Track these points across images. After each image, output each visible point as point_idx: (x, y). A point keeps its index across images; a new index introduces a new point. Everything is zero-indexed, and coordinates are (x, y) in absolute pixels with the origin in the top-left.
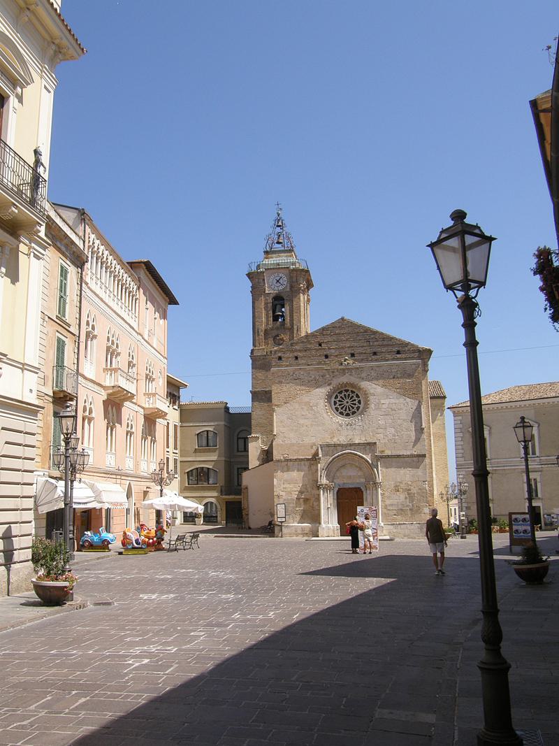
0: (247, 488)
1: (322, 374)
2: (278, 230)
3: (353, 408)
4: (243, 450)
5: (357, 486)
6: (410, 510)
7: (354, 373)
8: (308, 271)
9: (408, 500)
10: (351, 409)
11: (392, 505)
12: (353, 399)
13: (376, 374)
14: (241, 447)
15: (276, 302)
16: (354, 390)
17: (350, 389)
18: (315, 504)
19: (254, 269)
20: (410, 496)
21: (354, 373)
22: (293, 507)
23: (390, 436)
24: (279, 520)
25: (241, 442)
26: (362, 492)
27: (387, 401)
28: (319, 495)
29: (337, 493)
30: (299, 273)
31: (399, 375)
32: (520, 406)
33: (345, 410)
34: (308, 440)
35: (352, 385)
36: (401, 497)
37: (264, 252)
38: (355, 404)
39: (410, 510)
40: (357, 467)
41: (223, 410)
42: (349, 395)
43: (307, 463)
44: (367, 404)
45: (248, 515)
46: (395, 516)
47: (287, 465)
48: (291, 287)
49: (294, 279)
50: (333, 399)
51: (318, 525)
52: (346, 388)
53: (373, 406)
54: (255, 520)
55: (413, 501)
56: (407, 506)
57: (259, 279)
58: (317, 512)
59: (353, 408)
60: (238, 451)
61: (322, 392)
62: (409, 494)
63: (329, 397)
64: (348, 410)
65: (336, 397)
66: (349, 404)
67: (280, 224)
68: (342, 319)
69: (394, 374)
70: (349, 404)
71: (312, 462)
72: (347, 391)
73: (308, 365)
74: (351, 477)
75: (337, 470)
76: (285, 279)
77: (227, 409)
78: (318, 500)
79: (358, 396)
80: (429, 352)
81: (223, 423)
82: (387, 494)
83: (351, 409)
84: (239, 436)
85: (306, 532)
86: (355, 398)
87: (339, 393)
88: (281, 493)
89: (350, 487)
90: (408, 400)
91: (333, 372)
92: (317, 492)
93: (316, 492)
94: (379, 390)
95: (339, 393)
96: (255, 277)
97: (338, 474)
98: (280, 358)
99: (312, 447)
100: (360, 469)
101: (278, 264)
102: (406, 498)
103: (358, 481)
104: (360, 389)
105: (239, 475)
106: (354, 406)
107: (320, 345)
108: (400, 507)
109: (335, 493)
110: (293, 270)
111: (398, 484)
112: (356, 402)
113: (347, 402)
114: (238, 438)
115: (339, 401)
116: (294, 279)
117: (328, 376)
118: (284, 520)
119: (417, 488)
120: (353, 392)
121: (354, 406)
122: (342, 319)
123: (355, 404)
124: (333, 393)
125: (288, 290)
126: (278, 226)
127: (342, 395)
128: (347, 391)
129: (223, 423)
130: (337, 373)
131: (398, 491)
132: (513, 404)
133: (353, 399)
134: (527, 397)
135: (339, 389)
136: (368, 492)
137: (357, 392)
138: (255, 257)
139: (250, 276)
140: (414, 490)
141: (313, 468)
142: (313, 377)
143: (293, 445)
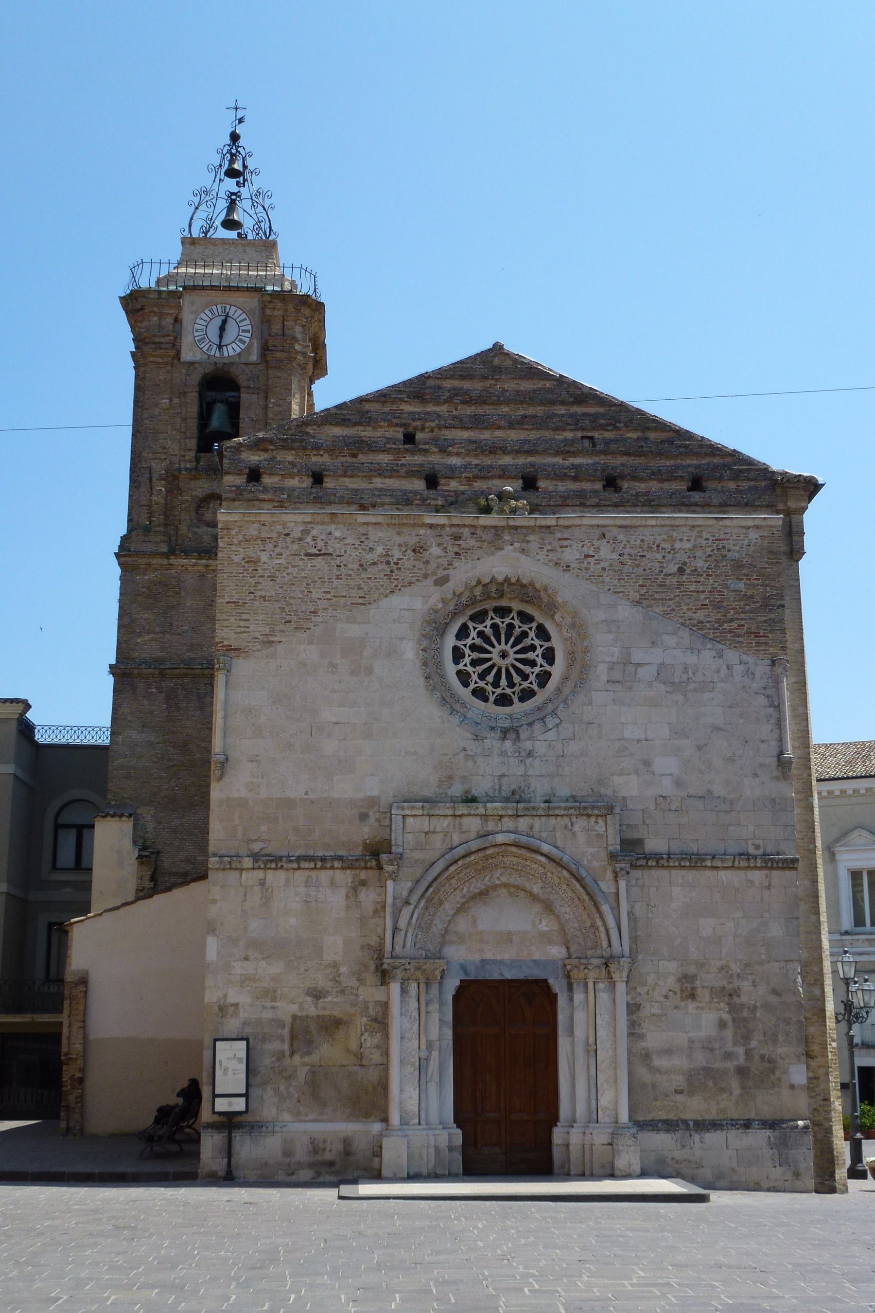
0: (83, 981)
1: (413, 541)
2: (230, 184)
3: (525, 677)
4: (72, 865)
5: (537, 973)
6: (742, 1072)
7: (534, 546)
8: (319, 307)
9: (729, 1033)
10: (517, 679)
11: (668, 1052)
12: (527, 642)
13: (615, 556)
14: (66, 857)
15: (211, 395)
16: (529, 610)
17: (516, 606)
18: (370, 1041)
19: (146, 281)
20: (741, 1021)
21: (534, 546)
22: (280, 1056)
23: (667, 786)
24: (221, 1105)
25: (68, 841)
26: (553, 999)
27: (656, 656)
28: (385, 1006)
29: (456, 998)
30: (290, 307)
31: (700, 564)
32: (854, 791)
33: (496, 684)
34: (344, 789)
35: (526, 591)
36: (704, 1020)
37: (184, 241)
38: (533, 664)
39: (742, 1072)
40: (534, 898)
41: (14, 726)
42: (511, 627)
43: (344, 878)
44: (581, 665)
45: (81, 1080)
46: (679, 1098)
47: (262, 883)
48: (265, 349)
49: (276, 328)
50: (450, 640)
51: (377, 1127)
52: (503, 603)
53: (601, 672)
54: (114, 1097)
55: (747, 1037)
56: (728, 1056)
57: (161, 316)
58: (373, 1075)
59: (525, 677)
60: (54, 867)
61: (405, 610)
62: (733, 1009)
63: (436, 627)
64: (504, 682)
65: (463, 633)
66: (512, 656)
67: (238, 166)
68: (497, 349)
69: (681, 557)
70: (511, 659)
71: (363, 875)
72: (503, 612)
73: (363, 507)
74: (507, 936)
75: (461, 909)
76: (246, 325)
77: (26, 729)
78: (381, 1022)
79: (543, 633)
80: (811, 487)
81: (10, 769)
82: (650, 1009)
83: (517, 679)
84: (62, 820)
85: (328, 1156)
86: (532, 638)
87: (473, 618)
88: (234, 996)
89: (509, 975)
90: (732, 656)
91: (457, 538)
92: (379, 994)
93: (371, 993)
94: (625, 612)
95: (473, 618)
96: (149, 312)
97: (462, 925)
98: (254, 475)
99: (363, 817)
100: (548, 908)
101: (228, 278)
102: (722, 1025)
103: (537, 956)
104: (551, 608)
105: (59, 934)
106: (527, 669)
107: (409, 438)
108: (701, 1059)
109: (449, 998)
110: (274, 294)
111: (692, 970)
112: (536, 655)
113: (504, 655)
114: (58, 827)
115: (473, 648)
116: (276, 328)
117: (435, 551)
118: (239, 1105)
119: (762, 989)
120: (526, 618)
121: (527, 669)
122: (497, 349)
123: (533, 664)
124: (455, 615)
125: (254, 358)
126: (232, 173)
127: (486, 627)
128: (503, 612)
129: (10, 769)
130: (472, 542)
131: (692, 996)
132: (849, 786)
133: (527, 642)
134: (860, 770)
135: (473, 601)
136: (578, 997)
137: (539, 618)
138: (158, 256)
139: (135, 304)
140: (751, 994)
141: (368, 897)
142: (380, 550)
143: (290, 803)
